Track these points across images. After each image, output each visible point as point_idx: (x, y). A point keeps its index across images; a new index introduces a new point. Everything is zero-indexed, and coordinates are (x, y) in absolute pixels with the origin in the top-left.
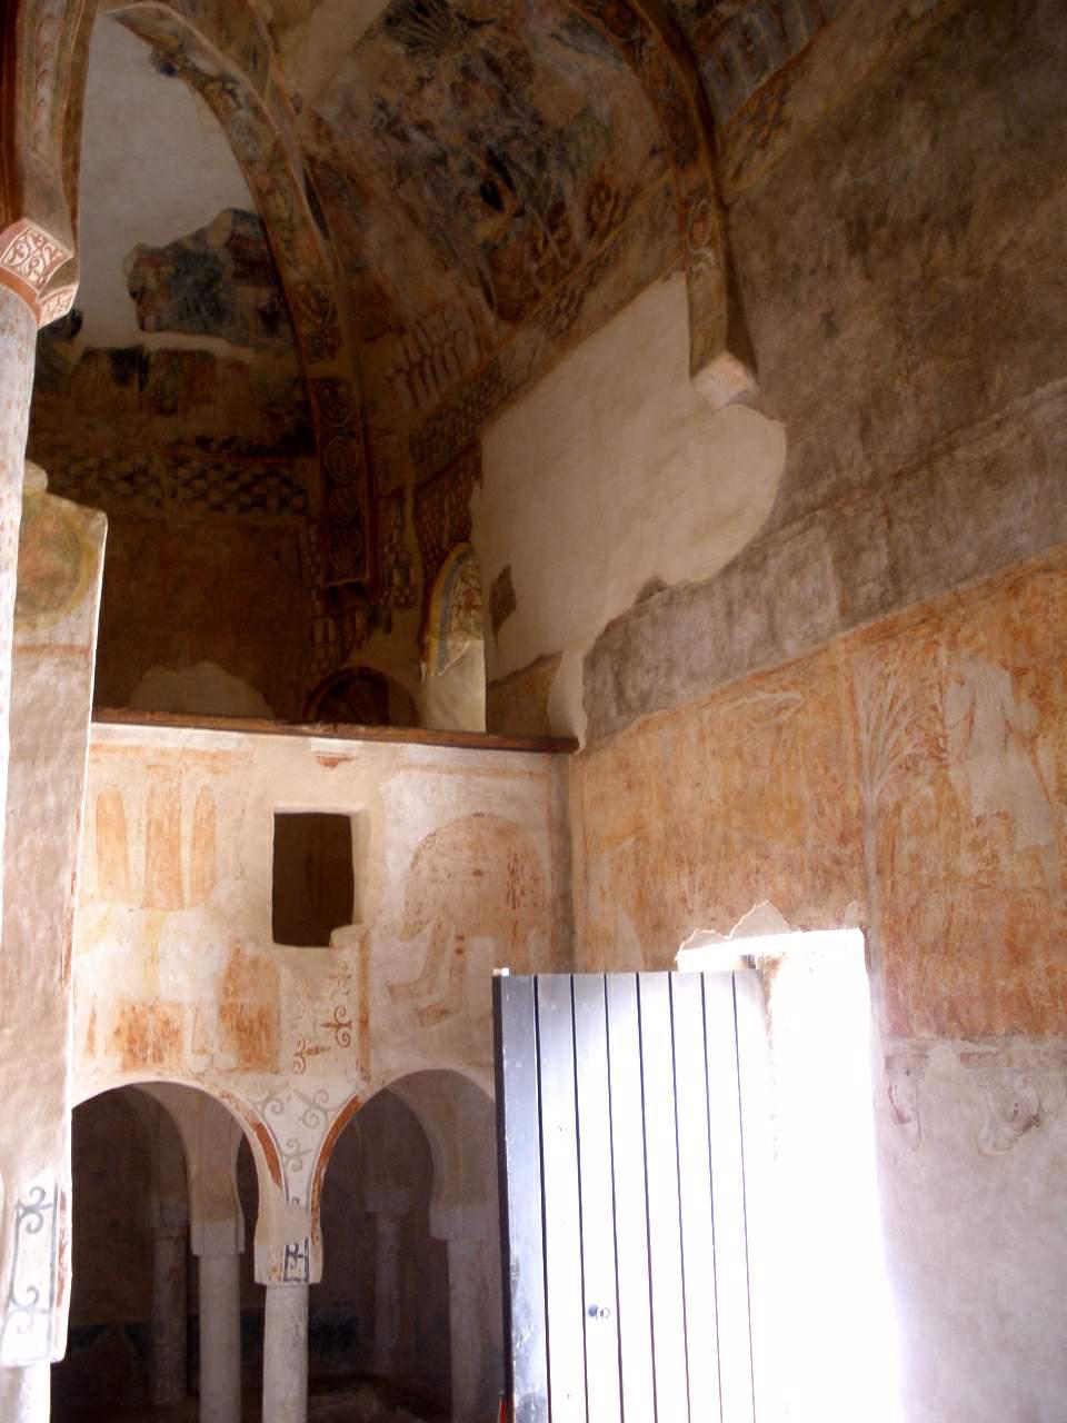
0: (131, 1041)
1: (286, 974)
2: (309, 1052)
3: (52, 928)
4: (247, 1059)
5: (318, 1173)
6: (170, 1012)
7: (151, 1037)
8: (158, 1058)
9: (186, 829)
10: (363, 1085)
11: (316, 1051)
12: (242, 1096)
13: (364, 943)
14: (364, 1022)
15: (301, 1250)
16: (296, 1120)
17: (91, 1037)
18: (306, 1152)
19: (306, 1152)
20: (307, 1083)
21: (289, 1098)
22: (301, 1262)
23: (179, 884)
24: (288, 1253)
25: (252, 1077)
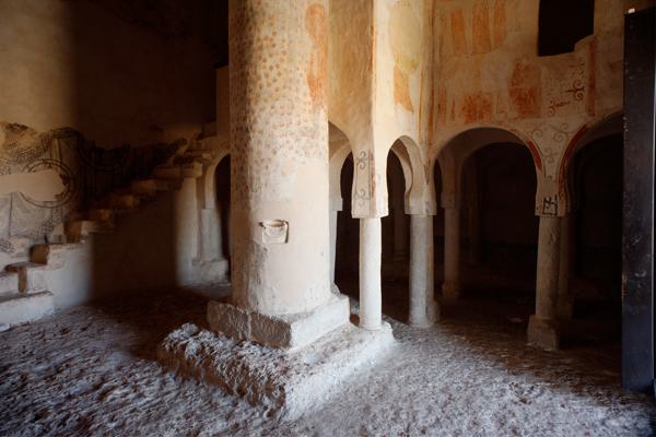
0: (469, 111)
1: (544, 71)
2: (558, 105)
3: (365, 52)
4: (524, 113)
5: (563, 165)
6: (487, 97)
7: (478, 109)
8: (481, 116)
9: (491, 14)
10: (590, 119)
11: (562, 105)
12: (523, 130)
13: (593, 45)
14: (592, 87)
15: (553, 201)
16: (550, 140)
17: (453, 112)
18: (556, 154)
19: (556, 154)
20: (556, 121)
21: (546, 129)
22: (553, 206)
23: (488, 40)
24: (545, 201)
25: (526, 121)
